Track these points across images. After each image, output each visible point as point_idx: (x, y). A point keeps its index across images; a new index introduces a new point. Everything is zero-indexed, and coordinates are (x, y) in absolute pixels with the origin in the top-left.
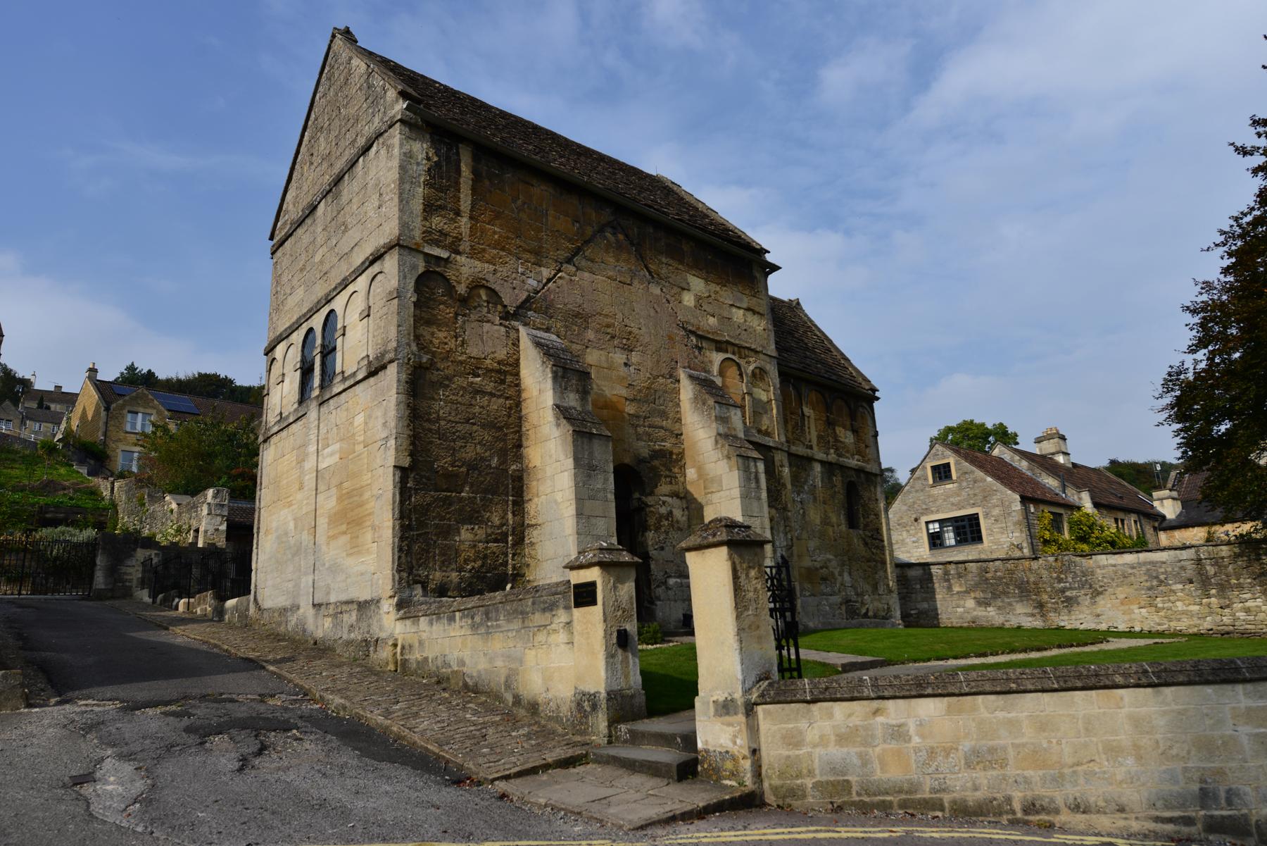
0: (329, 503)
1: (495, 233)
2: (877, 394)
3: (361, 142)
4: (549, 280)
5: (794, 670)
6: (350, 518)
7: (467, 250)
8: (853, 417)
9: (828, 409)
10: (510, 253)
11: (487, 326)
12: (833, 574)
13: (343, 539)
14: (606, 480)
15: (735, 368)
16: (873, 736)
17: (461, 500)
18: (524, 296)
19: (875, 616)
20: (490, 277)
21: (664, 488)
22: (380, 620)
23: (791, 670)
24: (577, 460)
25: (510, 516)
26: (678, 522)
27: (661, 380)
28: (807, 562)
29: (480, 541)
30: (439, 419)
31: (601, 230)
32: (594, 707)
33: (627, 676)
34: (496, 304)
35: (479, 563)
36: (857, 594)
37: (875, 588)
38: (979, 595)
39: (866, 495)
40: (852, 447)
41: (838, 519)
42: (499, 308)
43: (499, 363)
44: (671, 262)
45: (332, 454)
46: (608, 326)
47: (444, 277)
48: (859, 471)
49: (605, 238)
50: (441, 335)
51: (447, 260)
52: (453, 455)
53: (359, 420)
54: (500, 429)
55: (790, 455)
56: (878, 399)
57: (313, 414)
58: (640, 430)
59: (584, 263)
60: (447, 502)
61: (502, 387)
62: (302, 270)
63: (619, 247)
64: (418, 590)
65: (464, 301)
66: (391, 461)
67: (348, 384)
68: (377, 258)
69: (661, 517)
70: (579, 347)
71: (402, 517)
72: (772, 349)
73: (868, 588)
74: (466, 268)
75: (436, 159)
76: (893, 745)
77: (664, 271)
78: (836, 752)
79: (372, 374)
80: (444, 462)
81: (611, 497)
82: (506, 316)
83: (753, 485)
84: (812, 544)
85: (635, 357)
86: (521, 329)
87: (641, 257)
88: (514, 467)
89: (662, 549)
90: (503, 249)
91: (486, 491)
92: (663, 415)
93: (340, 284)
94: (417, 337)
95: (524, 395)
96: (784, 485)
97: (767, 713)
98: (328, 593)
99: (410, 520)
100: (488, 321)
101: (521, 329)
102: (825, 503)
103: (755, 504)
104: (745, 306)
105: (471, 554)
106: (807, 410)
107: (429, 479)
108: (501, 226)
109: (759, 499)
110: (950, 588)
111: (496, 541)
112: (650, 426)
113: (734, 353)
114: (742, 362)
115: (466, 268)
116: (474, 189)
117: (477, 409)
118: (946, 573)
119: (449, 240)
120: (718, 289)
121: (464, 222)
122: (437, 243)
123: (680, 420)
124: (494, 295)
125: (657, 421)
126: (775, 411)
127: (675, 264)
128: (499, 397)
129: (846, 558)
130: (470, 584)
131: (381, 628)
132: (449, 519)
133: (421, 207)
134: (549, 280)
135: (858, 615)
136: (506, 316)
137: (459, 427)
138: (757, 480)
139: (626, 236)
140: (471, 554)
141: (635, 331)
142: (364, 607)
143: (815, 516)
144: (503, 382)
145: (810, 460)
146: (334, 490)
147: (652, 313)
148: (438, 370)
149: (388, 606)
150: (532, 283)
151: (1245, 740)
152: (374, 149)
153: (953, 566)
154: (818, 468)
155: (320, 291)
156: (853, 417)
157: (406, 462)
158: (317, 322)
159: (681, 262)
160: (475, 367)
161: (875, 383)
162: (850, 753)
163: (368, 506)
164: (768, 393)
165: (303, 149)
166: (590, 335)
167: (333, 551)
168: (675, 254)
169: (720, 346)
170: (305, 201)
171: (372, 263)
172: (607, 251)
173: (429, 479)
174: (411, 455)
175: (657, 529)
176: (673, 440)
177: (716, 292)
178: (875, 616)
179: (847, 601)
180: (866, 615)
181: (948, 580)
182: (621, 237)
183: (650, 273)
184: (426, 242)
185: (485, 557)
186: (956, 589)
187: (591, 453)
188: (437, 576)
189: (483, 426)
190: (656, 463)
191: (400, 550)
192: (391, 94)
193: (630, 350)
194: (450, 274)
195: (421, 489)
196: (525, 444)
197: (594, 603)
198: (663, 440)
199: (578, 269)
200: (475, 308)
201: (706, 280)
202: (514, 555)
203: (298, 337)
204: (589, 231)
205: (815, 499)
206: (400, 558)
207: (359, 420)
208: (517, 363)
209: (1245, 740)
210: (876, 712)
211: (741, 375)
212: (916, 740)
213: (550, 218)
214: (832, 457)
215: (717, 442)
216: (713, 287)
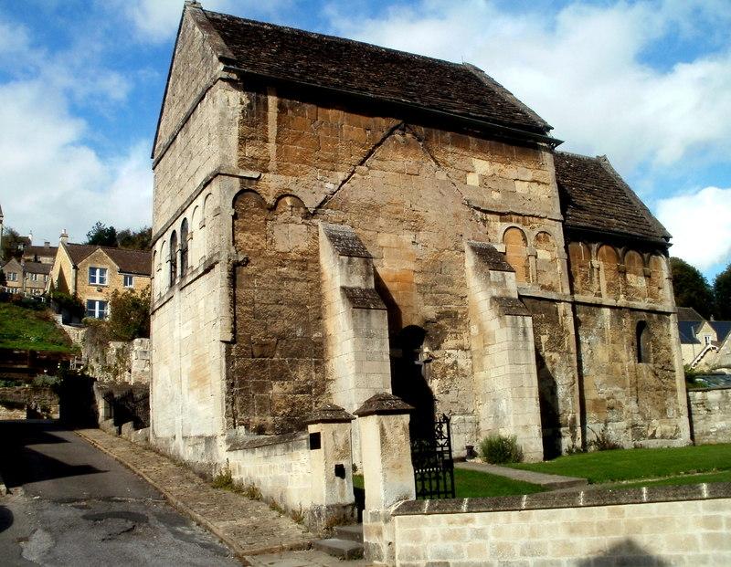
0: (187, 365)
1: (297, 150)
2: (671, 241)
3: (200, 91)
4: (344, 182)
5: (449, 492)
6: (199, 379)
7: (275, 168)
8: (646, 263)
9: (620, 259)
10: (310, 165)
11: (292, 226)
12: (620, 404)
13: (197, 391)
14: (382, 344)
15: (519, 233)
16: (465, 536)
17: (273, 363)
18: (322, 198)
19: (662, 437)
20: (293, 187)
21: (450, 343)
22: (217, 451)
23: (446, 492)
24: (356, 329)
25: (314, 373)
26: (462, 370)
27: (446, 252)
29: (289, 393)
30: (254, 303)
31: (391, 132)
32: (319, 514)
33: (342, 495)
34: (298, 207)
35: (289, 409)
36: (645, 419)
37: (664, 412)
39: (657, 332)
40: (644, 291)
41: (627, 356)
42: (302, 210)
43: (302, 254)
44: (455, 150)
45: (187, 328)
46: (397, 213)
47: (256, 192)
48: (651, 311)
49: (395, 139)
50: (254, 238)
51: (258, 179)
52: (265, 329)
53: (202, 304)
54: (304, 306)
55: (574, 304)
56: (671, 245)
57: (176, 297)
58: (428, 296)
59: (375, 163)
60: (262, 365)
61: (304, 273)
62: (169, 185)
63: (407, 144)
64: (242, 429)
65: (273, 208)
66: (218, 338)
67: (195, 276)
68: (207, 183)
69: (447, 366)
70: (371, 233)
71: (228, 378)
72: (556, 212)
73: (657, 413)
74: (272, 183)
75: (248, 102)
76: (477, 541)
77: (450, 159)
78: (441, 545)
79: (207, 271)
80: (258, 335)
81: (387, 357)
82: (308, 215)
84: (598, 380)
85: (422, 236)
86: (320, 224)
87: (428, 150)
88: (315, 335)
89: (448, 392)
90: (304, 162)
91: (292, 355)
92: (450, 282)
93: (188, 199)
94: (234, 242)
95: (323, 278)
96: (567, 332)
97: (401, 521)
98: (190, 430)
99: (234, 379)
100: (293, 222)
101: (320, 224)
102: (613, 342)
103: (522, 354)
104: (529, 178)
105: (283, 403)
106: (595, 263)
107: (246, 349)
108: (302, 145)
109: (526, 349)
111: (302, 392)
112: (437, 292)
113: (518, 222)
114: (526, 229)
115: (272, 183)
116: (279, 120)
117: (284, 293)
119: (260, 162)
120: (502, 167)
121: (272, 147)
122: (250, 167)
123: (465, 285)
124: (298, 202)
125: (443, 287)
126: (559, 268)
127: (460, 151)
128: (303, 281)
129: (634, 389)
130: (282, 425)
131: (218, 457)
132: (264, 378)
133: (237, 141)
134: (344, 182)
135: (645, 437)
136: (308, 215)
137: (270, 308)
138: (525, 333)
139: (414, 134)
140: (283, 403)
141: (422, 213)
142: (209, 440)
143: (602, 354)
144: (304, 269)
145: (600, 306)
146: (190, 355)
147: (438, 195)
148: (252, 265)
149: (221, 441)
150: (330, 186)
151: (700, 539)
152: (206, 99)
154: (607, 312)
155: (180, 202)
156: (646, 263)
157: (229, 337)
158: (177, 226)
159: (466, 149)
160: (282, 259)
161: (670, 230)
162: (450, 546)
163: (208, 369)
164: (551, 253)
165: (169, 90)
166: (381, 222)
167: (191, 400)
168: (456, 143)
169: (503, 216)
170: (171, 130)
171: (205, 186)
172: (396, 149)
173: (246, 349)
174: (234, 331)
175: (443, 376)
176: (459, 302)
177: (501, 171)
178: (662, 437)
179: (634, 426)
180: (653, 437)
182: (408, 136)
183: (436, 162)
184: (241, 167)
185: (294, 405)
188: (256, 420)
189: (290, 305)
190: (442, 322)
191: (227, 401)
192: (215, 58)
193: (417, 230)
194: (261, 187)
195: (242, 357)
196: (324, 316)
197: (319, 447)
198: (449, 303)
199: (370, 168)
200: (281, 213)
201: (490, 161)
202: (317, 403)
203: (168, 236)
204: (380, 136)
205: (604, 340)
206: (227, 407)
207: (202, 304)
208: (317, 253)
209: (700, 539)
210: (467, 521)
211: (525, 239)
212: (492, 539)
213: (344, 131)
214: (622, 301)
215: (491, 302)
216: (497, 166)
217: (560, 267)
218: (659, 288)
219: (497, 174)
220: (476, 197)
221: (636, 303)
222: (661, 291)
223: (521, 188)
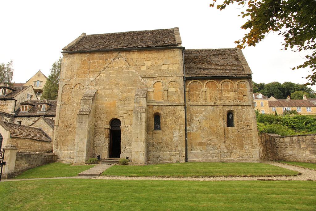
14: (85, 125)
28: (199, 140)
38: (311, 149)
72: (181, 73)
83: (139, 121)
104: (169, 63)
109: (141, 125)
110: (300, 146)
118: (298, 140)
138: (141, 119)
153: (301, 137)
181: (299, 143)
186: (302, 146)
187: (82, 120)
217: (180, 93)
218: (244, 96)
219: (154, 64)
220: (144, 74)
221: (229, 103)
222: (245, 97)
223: (164, 67)
